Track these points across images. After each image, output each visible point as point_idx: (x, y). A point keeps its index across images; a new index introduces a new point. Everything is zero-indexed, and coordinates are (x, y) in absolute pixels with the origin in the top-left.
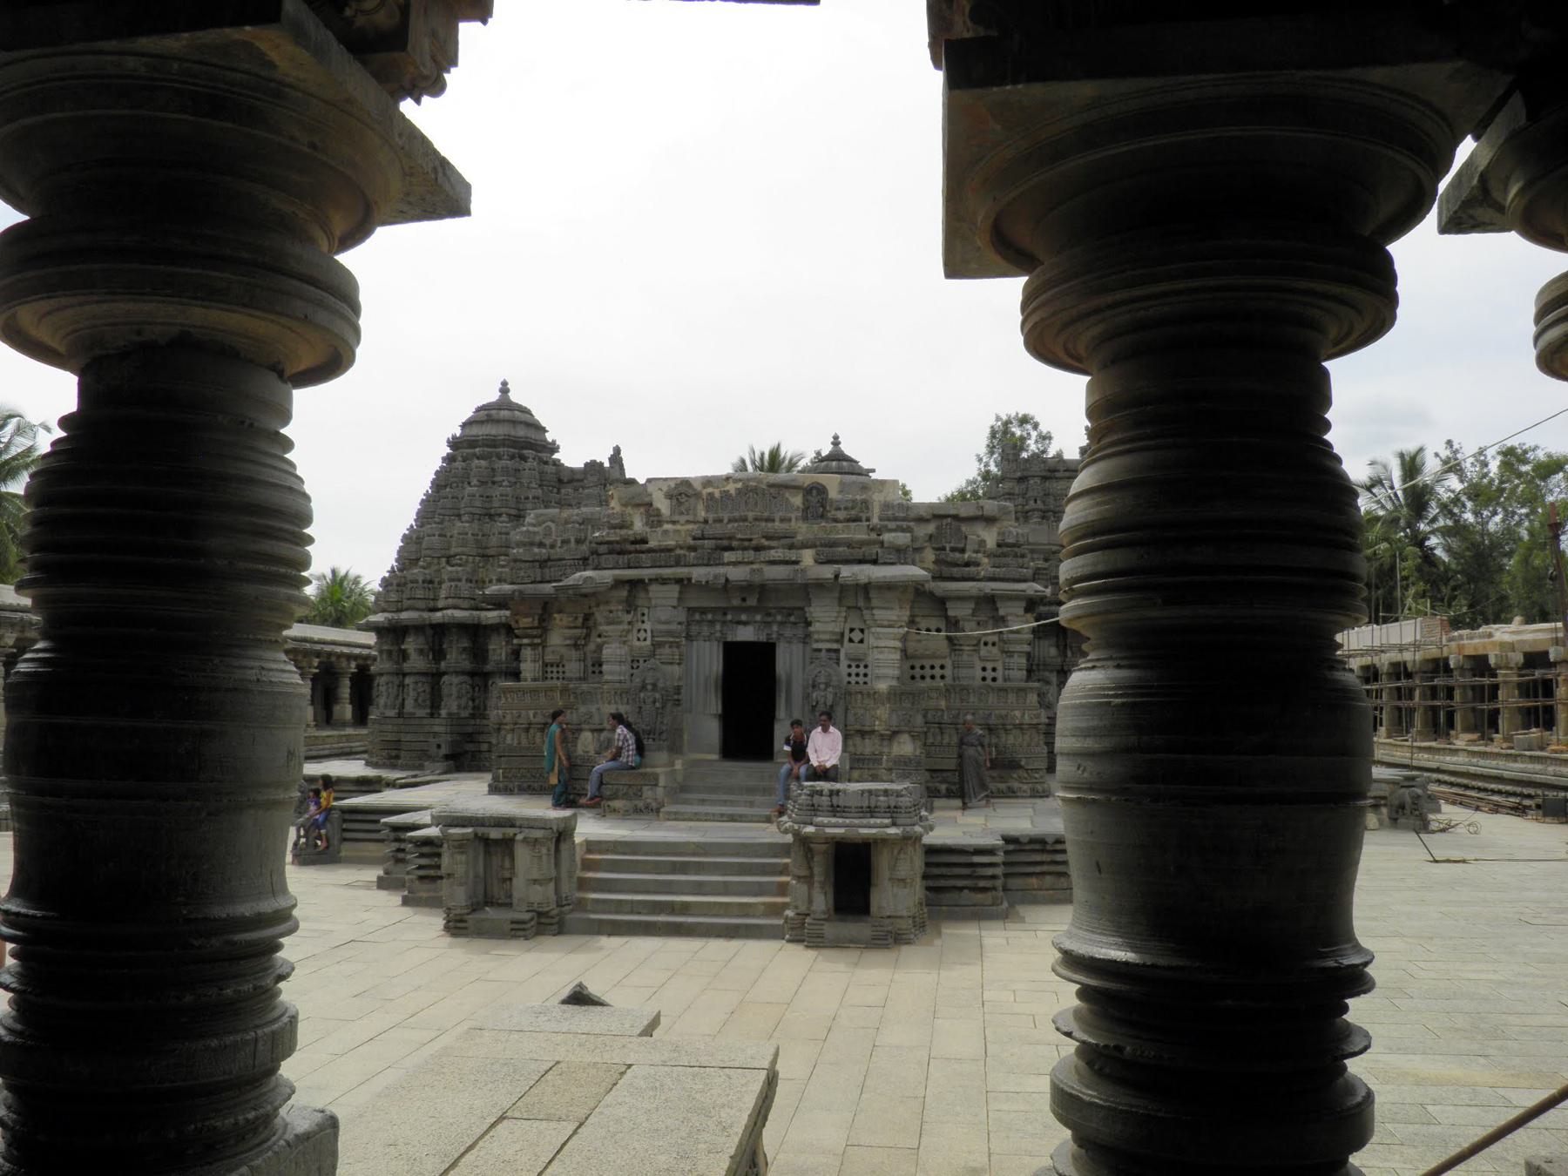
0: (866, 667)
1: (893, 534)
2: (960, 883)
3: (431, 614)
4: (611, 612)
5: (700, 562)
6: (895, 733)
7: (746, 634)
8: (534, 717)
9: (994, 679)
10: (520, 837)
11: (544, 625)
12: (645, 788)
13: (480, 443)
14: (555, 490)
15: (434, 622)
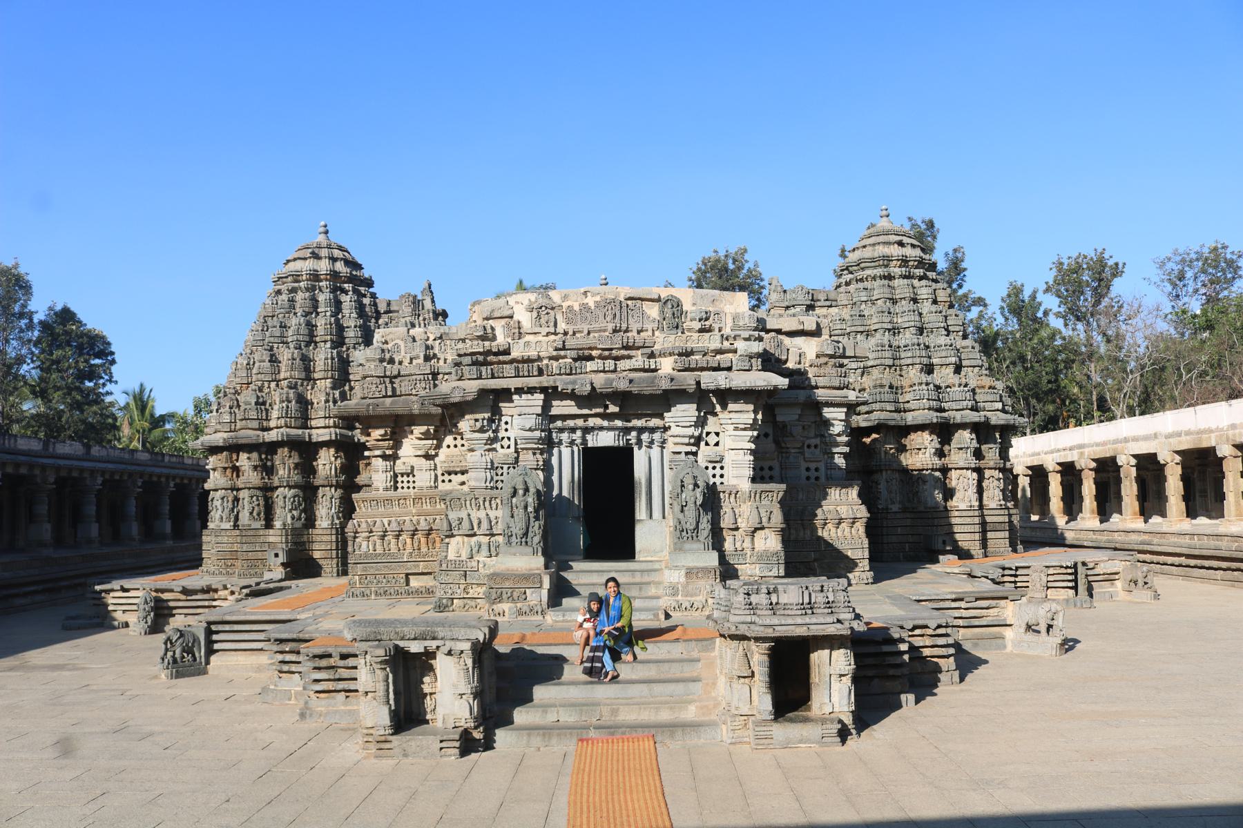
0: (722, 468)
1: (748, 343)
2: (870, 673)
3: (266, 433)
4: (477, 420)
5: (562, 372)
6: (756, 529)
7: (605, 439)
8: (389, 525)
9: (817, 478)
10: (445, 649)
11: (395, 437)
12: (527, 590)
13: (304, 278)
14: (373, 320)
15: (267, 440)
